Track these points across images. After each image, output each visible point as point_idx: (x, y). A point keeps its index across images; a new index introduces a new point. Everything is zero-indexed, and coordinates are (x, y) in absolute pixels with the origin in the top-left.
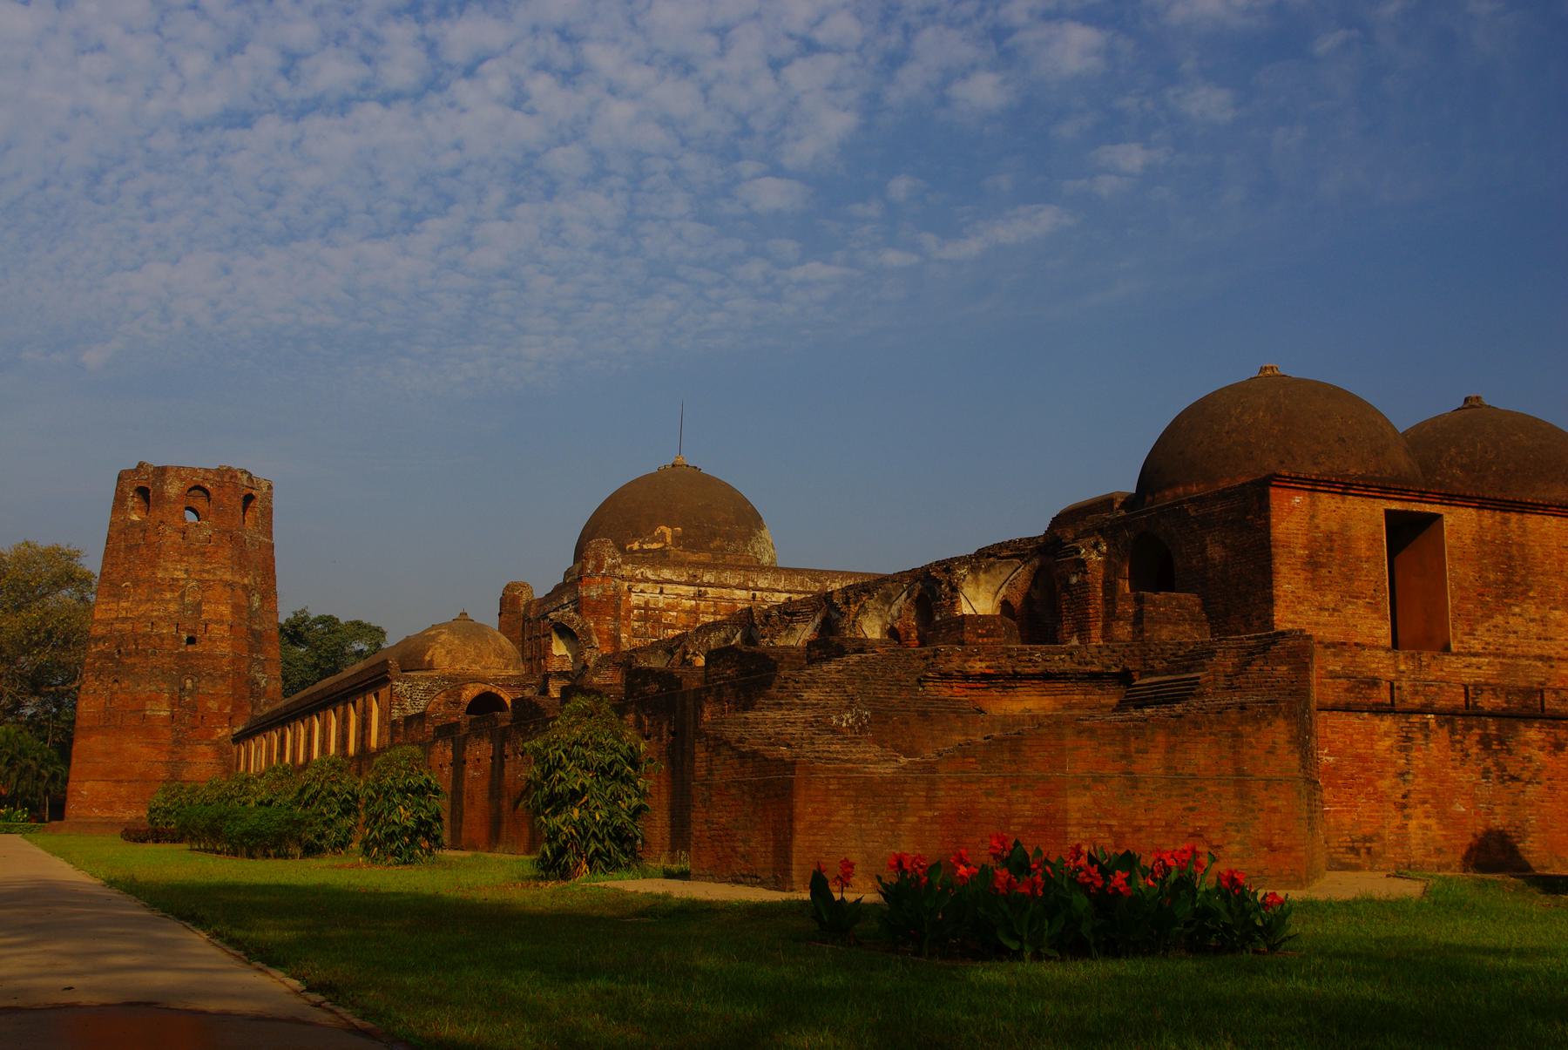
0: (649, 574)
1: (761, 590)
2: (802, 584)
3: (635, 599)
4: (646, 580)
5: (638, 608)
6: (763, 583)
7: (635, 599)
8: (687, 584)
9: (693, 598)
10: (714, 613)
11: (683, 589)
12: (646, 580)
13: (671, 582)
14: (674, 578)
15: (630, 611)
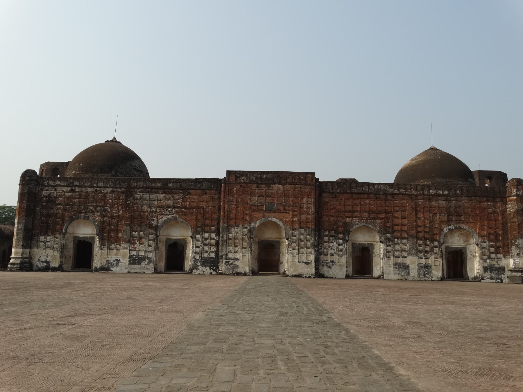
0: (51, 183)
1: (100, 187)
2: (119, 184)
3: (44, 193)
4: (49, 185)
5: (46, 197)
6: (101, 184)
7: (44, 193)
8: (67, 186)
9: (70, 192)
10: (80, 198)
11: (65, 189)
12: (49, 185)
13: (60, 186)
14: (61, 184)
15: (42, 198)
